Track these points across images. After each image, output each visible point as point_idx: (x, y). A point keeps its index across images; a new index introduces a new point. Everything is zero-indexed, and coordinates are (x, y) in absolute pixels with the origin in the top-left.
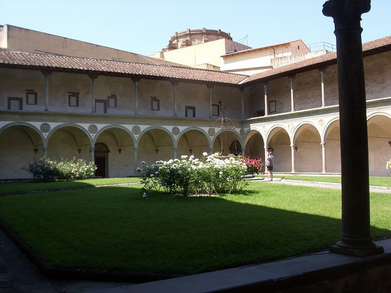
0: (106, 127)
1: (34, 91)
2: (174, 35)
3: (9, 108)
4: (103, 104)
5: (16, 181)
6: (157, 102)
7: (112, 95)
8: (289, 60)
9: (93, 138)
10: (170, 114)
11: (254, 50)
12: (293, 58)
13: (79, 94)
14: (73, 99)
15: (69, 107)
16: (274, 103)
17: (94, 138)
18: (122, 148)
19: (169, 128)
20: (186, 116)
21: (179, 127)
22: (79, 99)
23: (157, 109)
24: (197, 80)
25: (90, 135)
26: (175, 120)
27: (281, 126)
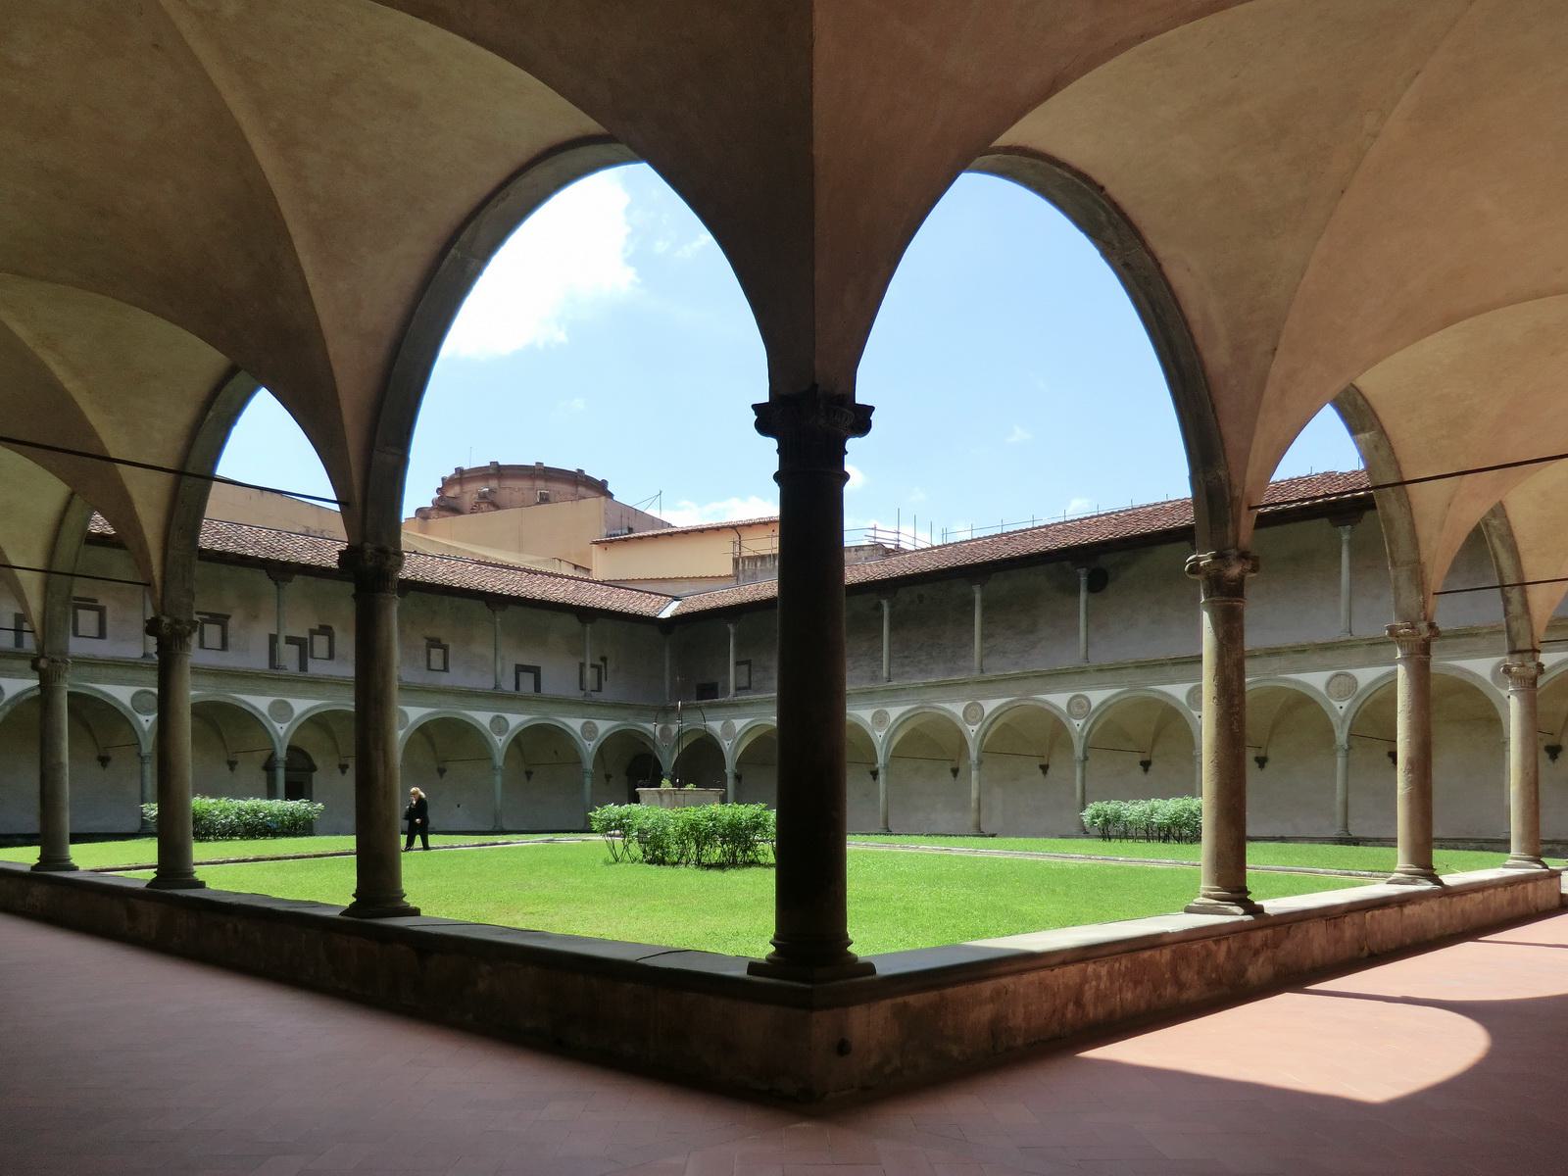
0: (316, 707)
2: (449, 472)
6: (441, 651)
11: (686, 533)
15: (202, 650)
16: (745, 668)
19: (482, 718)
20: (517, 687)
21: (508, 716)
24: (533, 599)
25: (272, 725)
26: (494, 697)
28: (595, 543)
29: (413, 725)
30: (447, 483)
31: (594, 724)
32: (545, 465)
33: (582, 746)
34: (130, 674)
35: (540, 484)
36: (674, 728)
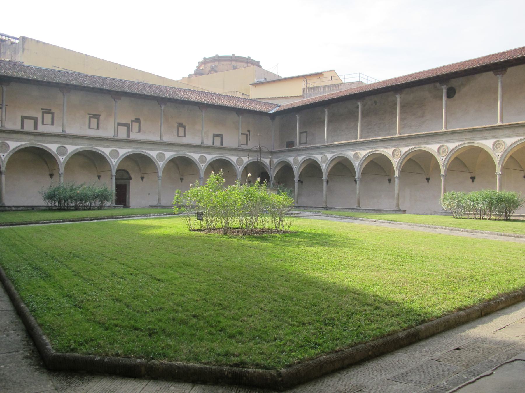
0: (128, 152)
1: (50, 110)
2: (201, 60)
3: (22, 127)
4: (126, 128)
5: (29, 208)
6: (183, 128)
7: (136, 119)
8: (322, 90)
9: (114, 163)
10: (197, 141)
12: (327, 88)
13: (100, 116)
14: (94, 121)
15: (90, 130)
16: (305, 134)
17: (116, 164)
18: (145, 176)
19: (195, 156)
20: (213, 143)
22: (100, 121)
23: (183, 135)
26: (202, 147)
27: (311, 158)
28: (251, 84)
29: (167, 159)
30: (201, 64)
31: (241, 159)
32: (236, 55)
33: (236, 168)
34: (56, 139)
35: (234, 63)
36: (275, 161)
